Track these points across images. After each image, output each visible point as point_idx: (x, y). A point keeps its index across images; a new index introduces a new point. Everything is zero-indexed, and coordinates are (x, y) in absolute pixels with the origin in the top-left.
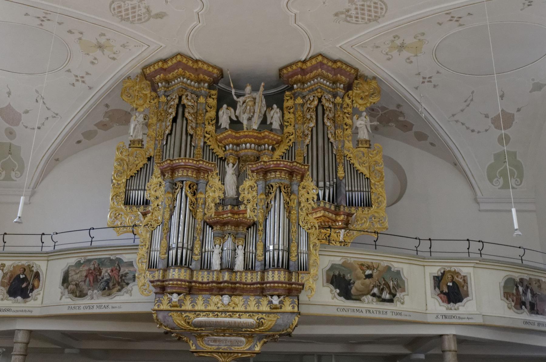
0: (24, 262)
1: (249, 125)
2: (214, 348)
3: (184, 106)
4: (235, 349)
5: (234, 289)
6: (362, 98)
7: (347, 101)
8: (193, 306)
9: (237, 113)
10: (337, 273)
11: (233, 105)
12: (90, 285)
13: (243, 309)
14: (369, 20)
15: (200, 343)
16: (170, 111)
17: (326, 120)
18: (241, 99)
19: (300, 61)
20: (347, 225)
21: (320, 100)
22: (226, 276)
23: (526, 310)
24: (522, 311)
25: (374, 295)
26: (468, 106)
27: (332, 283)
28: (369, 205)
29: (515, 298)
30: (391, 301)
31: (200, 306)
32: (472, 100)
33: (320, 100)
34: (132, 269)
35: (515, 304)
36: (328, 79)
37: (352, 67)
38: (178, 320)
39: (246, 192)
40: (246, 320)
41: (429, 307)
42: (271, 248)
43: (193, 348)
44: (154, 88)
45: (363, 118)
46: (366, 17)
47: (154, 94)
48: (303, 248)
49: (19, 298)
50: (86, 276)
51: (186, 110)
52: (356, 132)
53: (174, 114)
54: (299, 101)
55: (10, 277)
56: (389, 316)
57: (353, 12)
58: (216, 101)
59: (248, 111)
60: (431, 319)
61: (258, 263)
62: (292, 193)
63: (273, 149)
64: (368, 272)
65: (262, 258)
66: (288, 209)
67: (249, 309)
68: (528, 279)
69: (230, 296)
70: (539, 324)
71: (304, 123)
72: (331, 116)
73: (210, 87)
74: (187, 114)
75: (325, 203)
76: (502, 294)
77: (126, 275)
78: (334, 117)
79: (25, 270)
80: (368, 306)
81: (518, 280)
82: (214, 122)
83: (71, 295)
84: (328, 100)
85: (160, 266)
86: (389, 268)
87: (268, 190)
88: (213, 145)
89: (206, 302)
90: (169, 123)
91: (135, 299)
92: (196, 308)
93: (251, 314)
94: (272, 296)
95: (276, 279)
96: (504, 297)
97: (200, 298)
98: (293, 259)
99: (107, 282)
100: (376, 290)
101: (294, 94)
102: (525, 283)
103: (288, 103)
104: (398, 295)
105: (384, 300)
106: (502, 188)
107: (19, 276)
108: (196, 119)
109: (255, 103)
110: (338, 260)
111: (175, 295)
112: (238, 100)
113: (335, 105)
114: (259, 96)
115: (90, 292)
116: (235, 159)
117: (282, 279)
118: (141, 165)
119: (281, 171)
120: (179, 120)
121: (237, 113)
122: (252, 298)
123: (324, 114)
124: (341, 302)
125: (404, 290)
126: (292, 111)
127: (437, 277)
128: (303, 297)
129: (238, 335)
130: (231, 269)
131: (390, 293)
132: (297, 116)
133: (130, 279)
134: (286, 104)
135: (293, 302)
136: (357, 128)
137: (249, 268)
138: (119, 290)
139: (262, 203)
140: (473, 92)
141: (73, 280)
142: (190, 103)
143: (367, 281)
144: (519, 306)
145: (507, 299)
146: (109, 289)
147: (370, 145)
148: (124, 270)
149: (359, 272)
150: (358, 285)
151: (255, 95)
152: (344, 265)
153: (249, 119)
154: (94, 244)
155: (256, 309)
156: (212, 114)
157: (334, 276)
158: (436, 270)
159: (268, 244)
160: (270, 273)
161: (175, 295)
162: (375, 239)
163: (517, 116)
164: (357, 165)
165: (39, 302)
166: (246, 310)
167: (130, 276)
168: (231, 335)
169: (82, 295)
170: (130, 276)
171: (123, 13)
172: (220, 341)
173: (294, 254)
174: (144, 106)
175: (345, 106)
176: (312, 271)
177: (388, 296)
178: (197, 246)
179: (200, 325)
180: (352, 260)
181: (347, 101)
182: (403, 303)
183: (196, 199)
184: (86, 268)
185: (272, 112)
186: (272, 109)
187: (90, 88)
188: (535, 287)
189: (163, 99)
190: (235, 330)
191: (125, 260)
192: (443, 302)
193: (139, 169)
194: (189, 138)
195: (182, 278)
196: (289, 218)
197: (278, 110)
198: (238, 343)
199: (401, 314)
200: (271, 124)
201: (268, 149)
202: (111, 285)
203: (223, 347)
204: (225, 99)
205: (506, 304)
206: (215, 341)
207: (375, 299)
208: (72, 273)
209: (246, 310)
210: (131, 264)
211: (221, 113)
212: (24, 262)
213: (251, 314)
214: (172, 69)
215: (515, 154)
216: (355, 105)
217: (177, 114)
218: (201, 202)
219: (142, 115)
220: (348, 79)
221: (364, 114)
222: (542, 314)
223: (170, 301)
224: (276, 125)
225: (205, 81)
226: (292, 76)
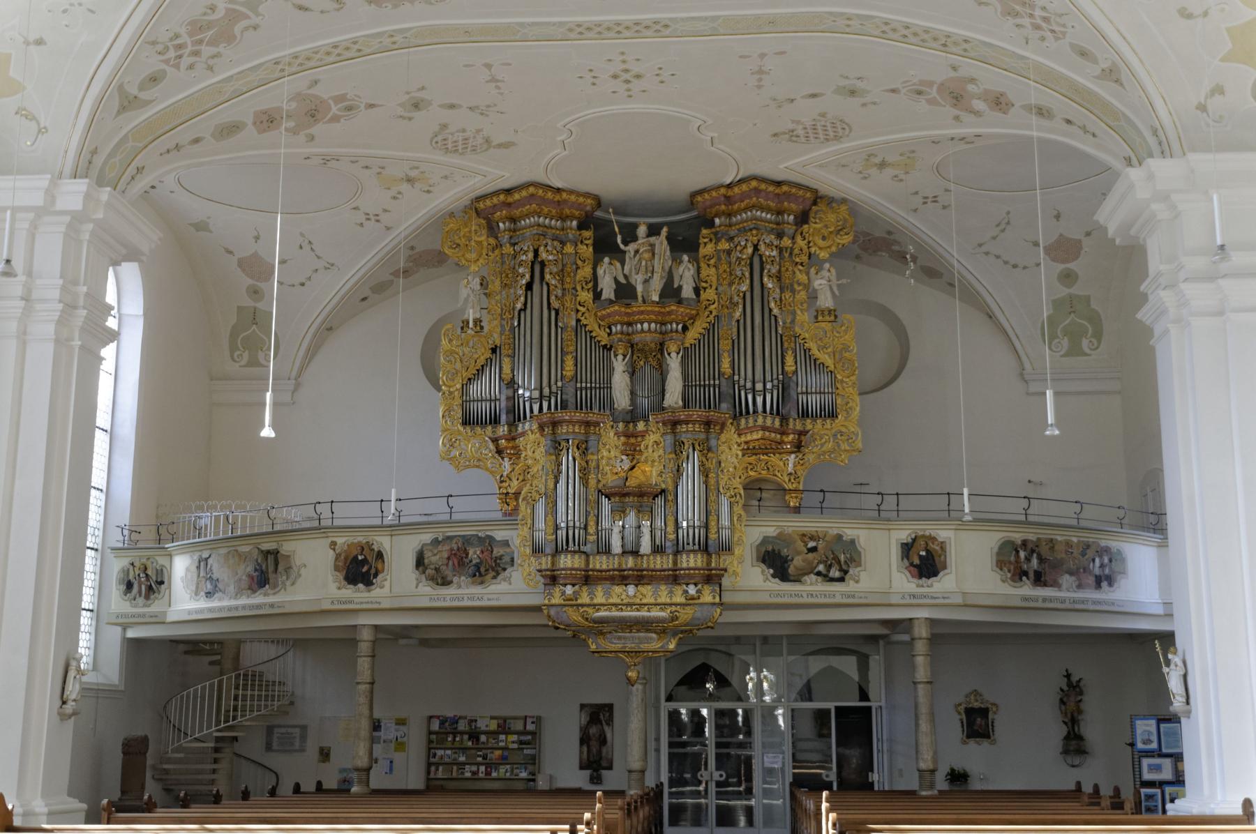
0: (360, 539)
1: (646, 290)
2: (617, 646)
3: (543, 264)
4: (644, 647)
5: (640, 578)
6: (824, 238)
7: (801, 243)
8: (592, 599)
9: (626, 271)
10: (770, 548)
11: (619, 255)
12: (454, 570)
13: (652, 601)
14: (827, 140)
15: (601, 641)
16: (521, 270)
17: (765, 279)
18: (631, 248)
19: (722, 186)
20: (798, 447)
21: (756, 248)
22: (630, 562)
25: (819, 574)
26: (1003, 231)
27: (764, 561)
28: (833, 415)
30: (841, 580)
31: (600, 598)
32: (1008, 223)
33: (756, 248)
34: (508, 550)
35: (1013, 575)
36: (769, 210)
37: (807, 188)
38: (574, 616)
39: (650, 450)
40: (656, 613)
41: (894, 584)
42: (685, 524)
43: (593, 647)
44: (492, 229)
45: (825, 273)
46: (821, 136)
47: (492, 241)
48: (725, 522)
49: (361, 586)
50: (448, 558)
51: (547, 270)
52: (813, 296)
53: (528, 276)
54: (724, 245)
55: (346, 559)
56: (838, 600)
57: (800, 132)
58: (591, 249)
59: (643, 269)
60: (895, 600)
61: (668, 544)
62: (709, 450)
63: (685, 328)
64: (811, 544)
65: (673, 537)
66: (705, 473)
67: (659, 601)
69: (636, 586)
70: (1044, 600)
71: (730, 284)
72: (774, 271)
73: (580, 227)
74: (548, 277)
75: (765, 418)
77: (500, 558)
78: (779, 271)
79: (363, 549)
80: (812, 588)
82: (590, 285)
83: (430, 583)
84: (770, 245)
85: (548, 550)
86: (839, 537)
87: (678, 447)
88: (590, 322)
89: (607, 594)
90: (521, 292)
91: (517, 587)
92: (595, 601)
93: (663, 606)
94: (687, 584)
95: (692, 565)
97: (599, 588)
98: (713, 536)
99: (478, 566)
100: (821, 568)
101: (716, 234)
102: (1030, 546)
103: (706, 249)
104: (851, 571)
105: (832, 580)
106: (1066, 355)
107: (356, 557)
108: (562, 281)
109: (653, 254)
110: (771, 531)
111: (569, 587)
112: (627, 248)
113: (781, 250)
114: (661, 243)
115: (455, 579)
116: (626, 348)
117: (699, 564)
118: (482, 361)
119: (694, 422)
120: (536, 287)
121: (626, 271)
122: (663, 587)
123: (762, 270)
124: (776, 585)
125: (860, 565)
126: (712, 262)
127: (906, 544)
128: (726, 582)
129: (648, 631)
130: (635, 553)
131: (841, 570)
132: (721, 271)
133: (506, 563)
134: (703, 251)
135: (713, 591)
136: (815, 291)
137: (658, 550)
138: (494, 577)
139: (671, 465)
140: (1008, 213)
141: (431, 563)
142: (551, 257)
143: (810, 555)
146: (481, 575)
147: (836, 317)
148: (498, 551)
149: (800, 545)
150: (798, 562)
151: (652, 239)
152: (780, 537)
153: (646, 281)
154: (455, 517)
155: (668, 601)
156: (586, 271)
157: (767, 552)
158: (904, 535)
159: (680, 519)
160: (684, 556)
161: (569, 587)
162: (823, 498)
163: (1086, 242)
164: (815, 351)
165: (386, 590)
166: (656, 601)
167: (506, 559)
168: (638, 631)
169: (446, 583)
170: (506, 559)
171: (450, 146)
172: (625, 638)
173: (713, 530)
174: (479, 263)
175: (796, 251)
176: (737, 551)
177: (837, 574)
178: (592, 523)
179: (602, 621)
180: (790, 529)
181: (801, 243)
182: (857, 582)
183: (587, 462)
184: (447, 547)
185: (681, 269)
186: (681, 262)
187: (388, 229)
188: (1044, 550)
189: (508, 249)
190: (645, 625)
191: (498, 539)
192: (913, 576)
193: (479, 367)
194: (553, 313)
195: (576, 566)
196: (706, 483)
197: (690, 266)
198: (648, 640)
199: (853, 596)
200: (680, 287)
201: (677, 331)
202: (482, 570)
203: (630, 646)
204: (606, 247)
206: (619, 638)
207: (820, 579)
208: (427, 554)
209: (656, 601)
210: (506, 543)
211: (600, 271)
212: (360, 538)
213: (663, 606)
214: (520, 203)
215: (1087, 299)
216: (813, 250)
217: (532, 277)
218: (592, 465)
219: (478, 280)
220: (800, 205)
221: (827, 265)
223: (563, 593)
224: (688, 292)
225: (572, 218)
226: (711, 207)
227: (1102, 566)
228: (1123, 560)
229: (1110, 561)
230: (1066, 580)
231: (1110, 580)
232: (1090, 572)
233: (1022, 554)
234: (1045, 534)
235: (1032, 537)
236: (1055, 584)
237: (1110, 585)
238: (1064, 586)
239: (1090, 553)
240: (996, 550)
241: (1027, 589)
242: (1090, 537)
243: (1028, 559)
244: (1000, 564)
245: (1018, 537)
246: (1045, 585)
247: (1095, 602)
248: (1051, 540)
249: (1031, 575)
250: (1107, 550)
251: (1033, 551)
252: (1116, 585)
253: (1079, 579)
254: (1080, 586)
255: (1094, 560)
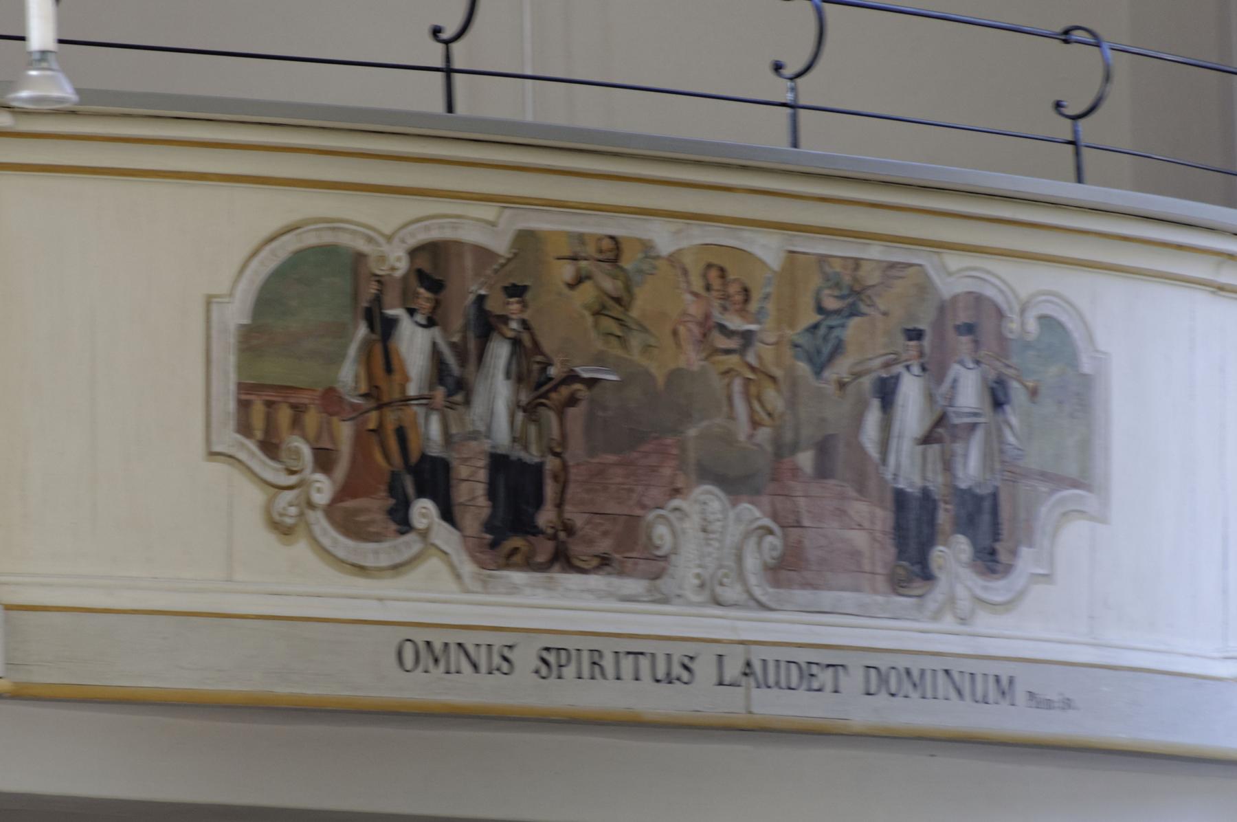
23: (443, 534)
24: (409, 545)
29: (345, 431)
35: (345, 492)
68: (501, 245)
76: (227, 403)
81: (397, 262)
96: (245, 428)
144: (375, 505)
145: (270, 447)
188: (563, 319)
205: (254, 496)
222: (604, 563)
227: (940, 431)
228: (1080, 396)
229: (998, 398)
230: (702, 525)
231: (991, 530)
232: (862, 477)
233: (414, 344)
234: (577, 206)
235: (483, 229)
236: (625, 551)
237: (990, 560)
238: (687, 569)
239: (866, 344)
240: (236, 313)
241: (439, 585)
242: (866, 235)
243: (453, 382)
244: (266, 409)
245: (386, 229)
246: (563, 559)
247: (887, 676)
248: (613, 250)
249: (472, 487)
250: (976, 322)
251: (486, 325)
252: (1027, 562)
253: (787, 522)
254: (788, 568)
255: (886, 392)
